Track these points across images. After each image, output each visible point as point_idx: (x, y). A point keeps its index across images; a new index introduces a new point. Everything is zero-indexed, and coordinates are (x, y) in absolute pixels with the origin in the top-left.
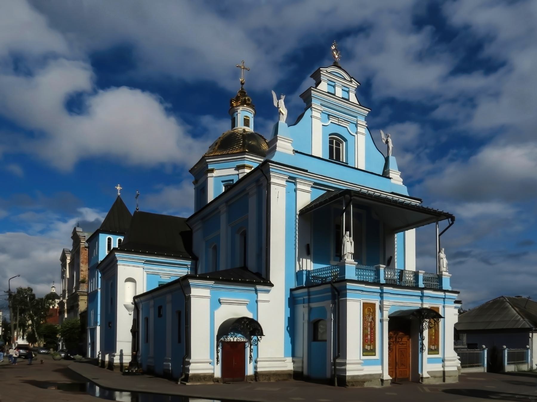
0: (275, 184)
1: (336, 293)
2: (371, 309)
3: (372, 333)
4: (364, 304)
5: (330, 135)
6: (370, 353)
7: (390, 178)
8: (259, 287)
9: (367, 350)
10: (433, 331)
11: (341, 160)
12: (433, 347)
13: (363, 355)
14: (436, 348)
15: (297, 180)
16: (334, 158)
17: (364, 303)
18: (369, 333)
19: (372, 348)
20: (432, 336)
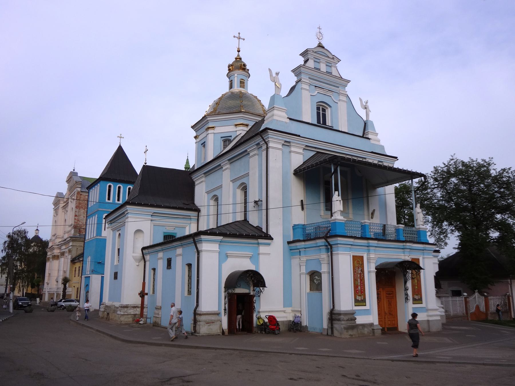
0: (273, 148)
1: (329, 247)
2: (360, 261)
4: (354, 257)
5: (317, 103)
6: (361, 304)
7: (370, 139)
8: (260, 241)
9: (358, 300)
10: (416, 280)
11: (327, 125)
12: (416, 297)
14: (419, 298)
15: (291, 144)
16: (321, 123)
17: (353, 256)
18: (359, 284)
19: (362, 299)
20: (415, 286)
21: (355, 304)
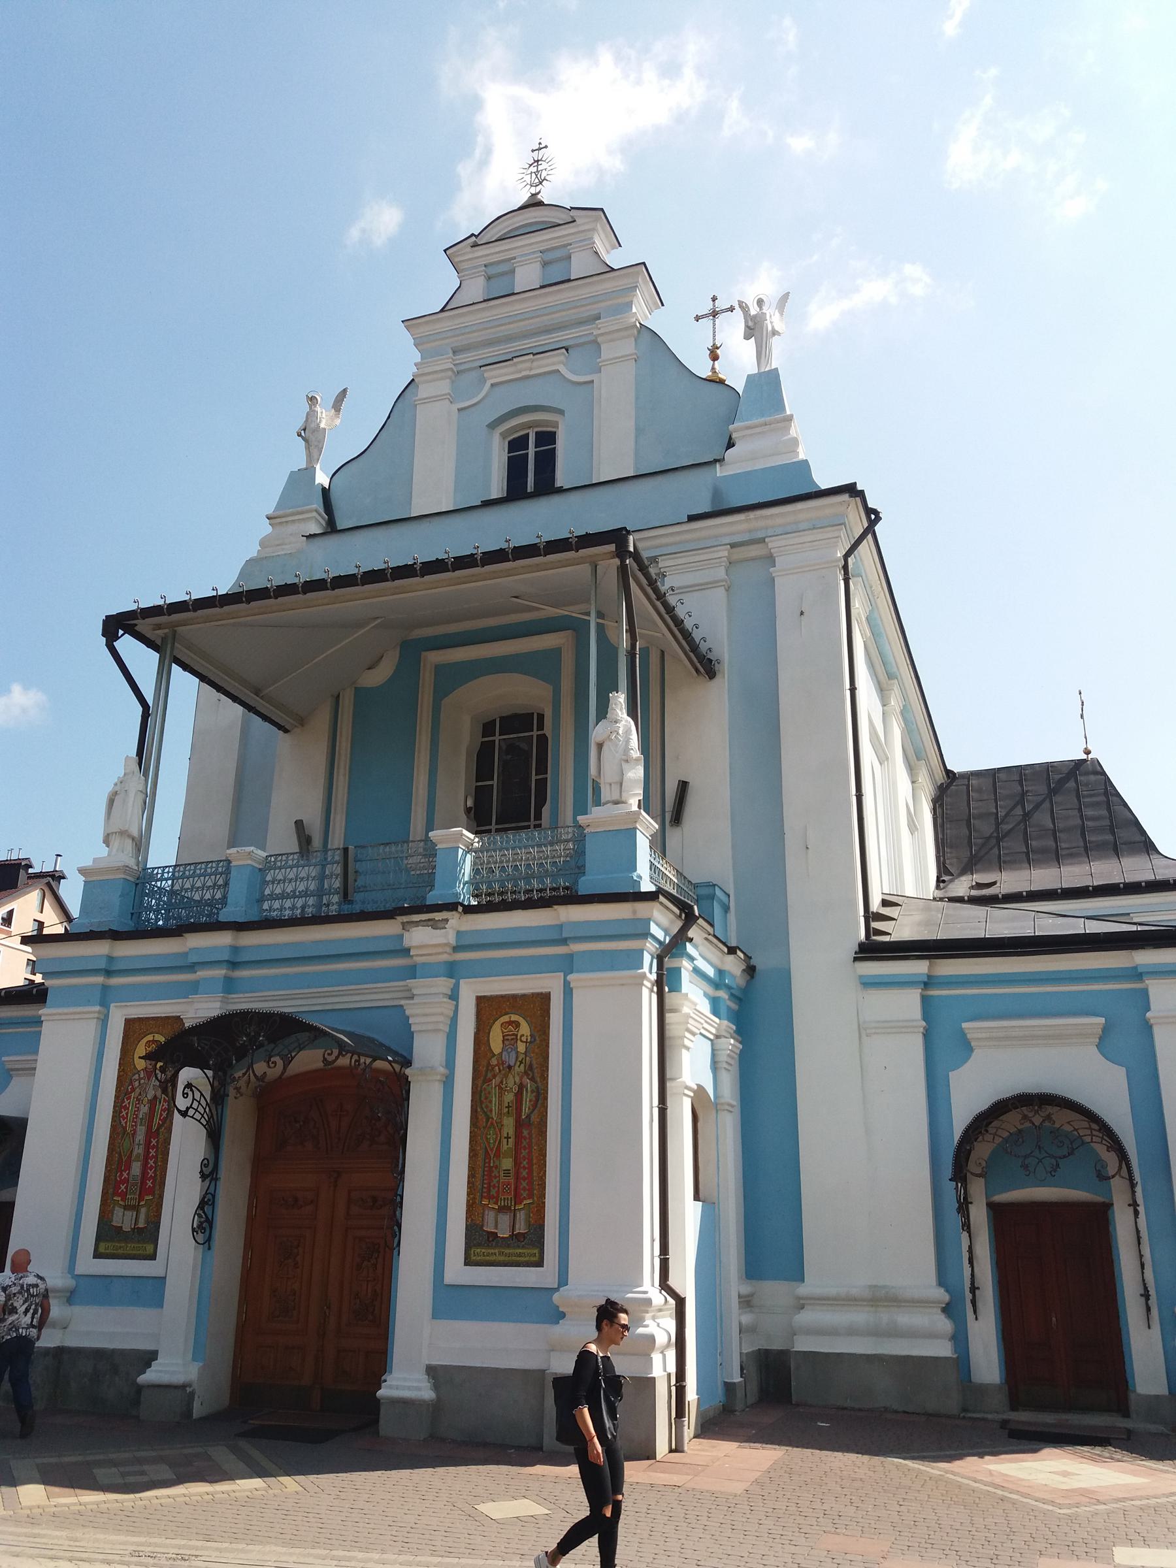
3: (152, 1152)
6: (130, 1248)
13: (97, 1255)
14: (521, 1228)
18: (139, 1151)
19: (141, 1225)
21: (96, 1250)
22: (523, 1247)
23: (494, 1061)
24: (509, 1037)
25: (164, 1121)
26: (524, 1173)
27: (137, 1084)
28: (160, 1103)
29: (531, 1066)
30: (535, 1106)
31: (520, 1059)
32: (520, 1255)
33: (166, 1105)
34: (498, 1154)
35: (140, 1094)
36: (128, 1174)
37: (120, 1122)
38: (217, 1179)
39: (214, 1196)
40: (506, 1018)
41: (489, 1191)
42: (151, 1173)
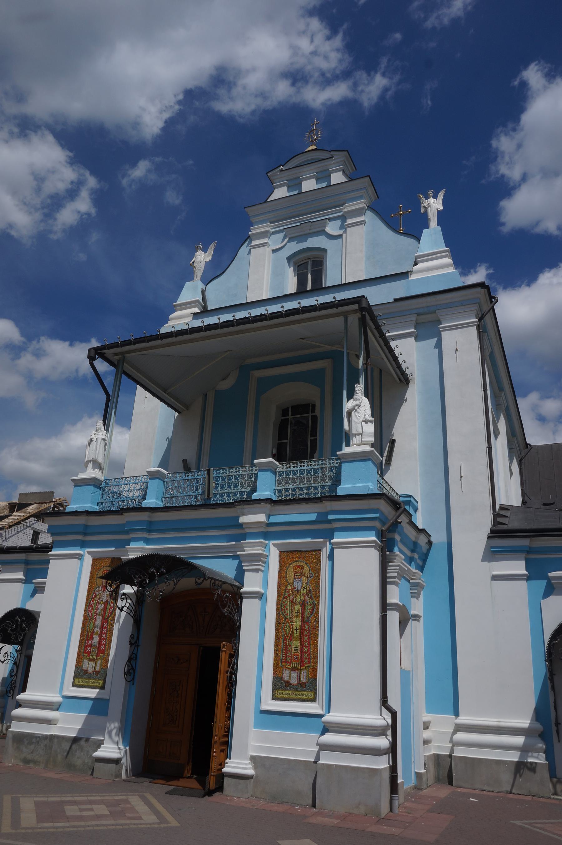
3: (105, 631)
9: (86, 672)
14: (304, 679)
18: (98, 629)
19: (98, 669)
21: (73, 682)
22: (305, 691)
23: (289, 587)
24: (298, 574)
25: (111, 613)
26: (306, 649)
27: (97, 593)
28: (109, 604)
29: (310, 590)
30: (312, 613)
31: (304, 586)
32: (303, 695)
33: (112, 605)
34: (291, 639)
35: (99, 599)
36: (92, 642)
37: (88, 613)
38: (138, 646)
39: (136, 655)
40: (296, 564)
41: (286, 659)
42: (103, 642)
